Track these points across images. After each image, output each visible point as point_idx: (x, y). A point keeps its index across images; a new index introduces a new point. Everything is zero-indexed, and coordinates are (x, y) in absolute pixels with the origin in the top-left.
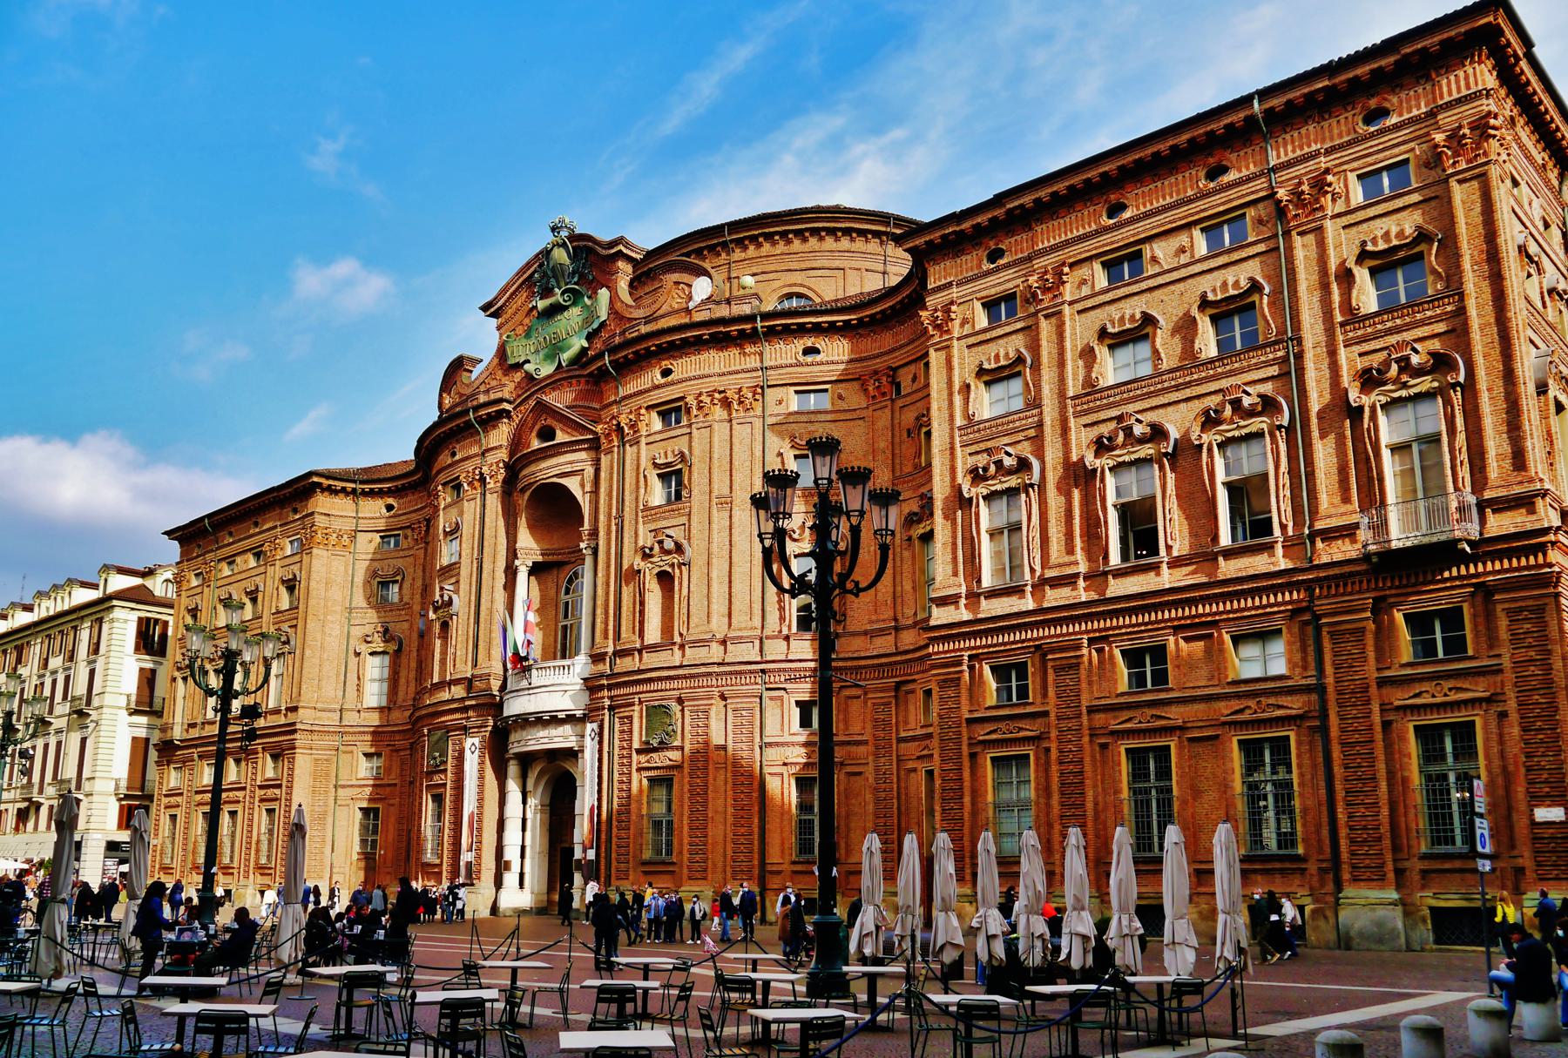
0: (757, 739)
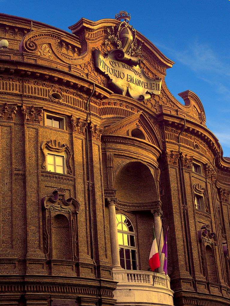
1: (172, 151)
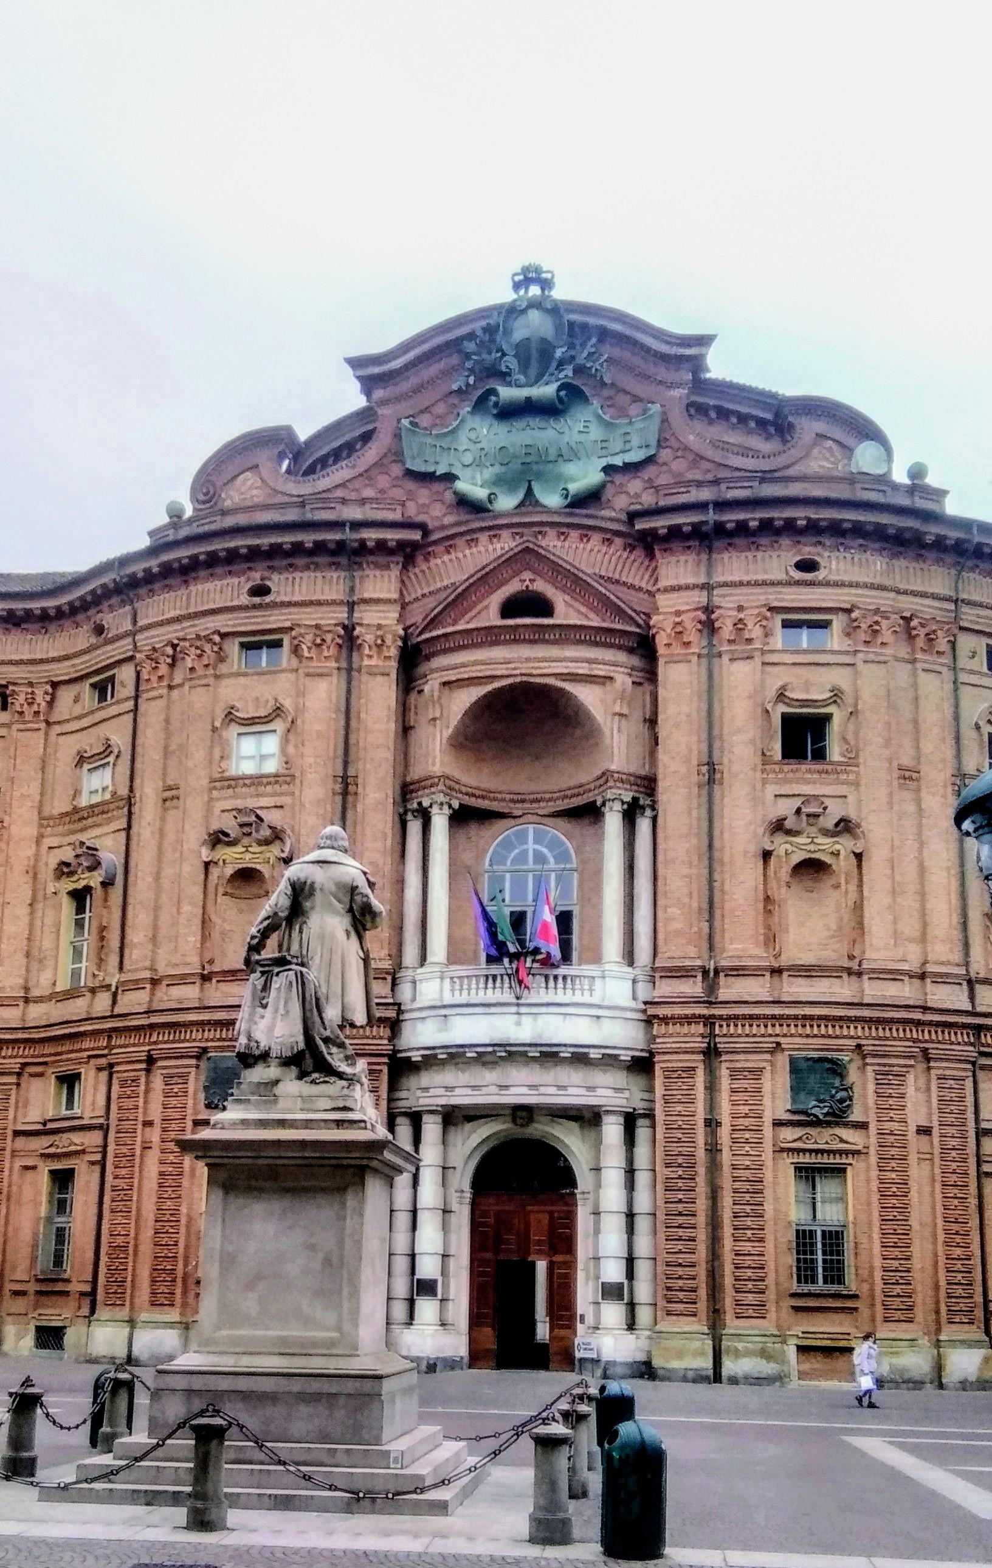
0: (971, 1123)
1: (678, 613)
